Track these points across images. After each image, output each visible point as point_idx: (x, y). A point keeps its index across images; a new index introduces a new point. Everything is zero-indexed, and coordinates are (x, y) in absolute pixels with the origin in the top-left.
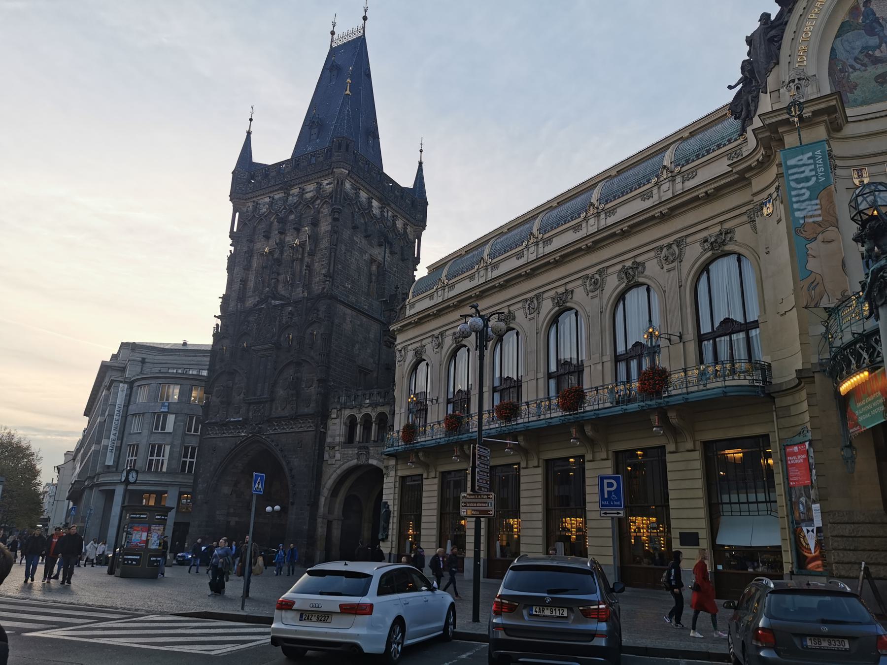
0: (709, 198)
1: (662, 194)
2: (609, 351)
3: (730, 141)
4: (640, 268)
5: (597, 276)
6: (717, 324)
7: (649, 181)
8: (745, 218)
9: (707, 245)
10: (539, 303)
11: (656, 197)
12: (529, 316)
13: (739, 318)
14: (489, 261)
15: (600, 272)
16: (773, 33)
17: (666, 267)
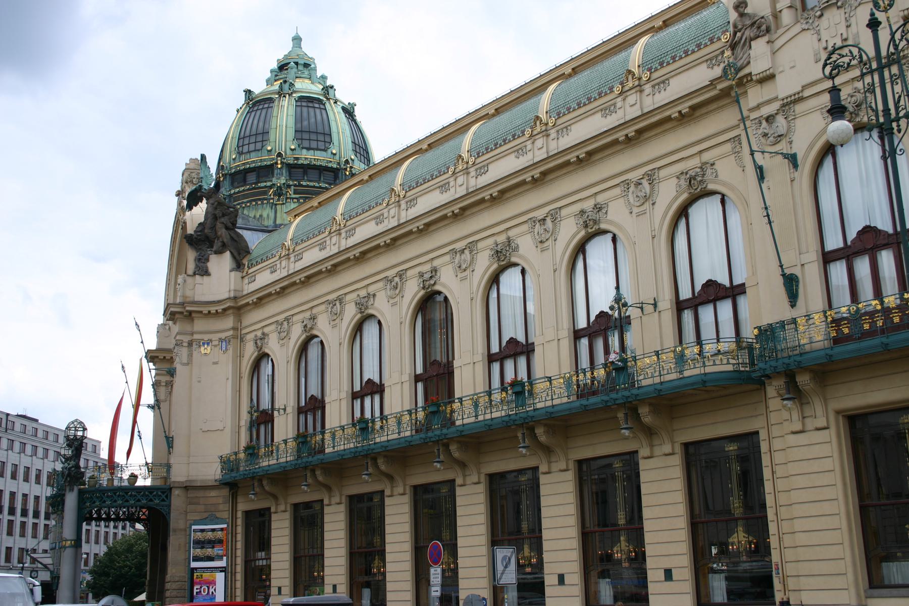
0: (684, 119)
1: (627, 106)
2: (566, 324)
6: (698, 288)
7: (611, 89)
8: (728, 147)
12: (460, 275)
14: (402, 194)
17: (635, 210)
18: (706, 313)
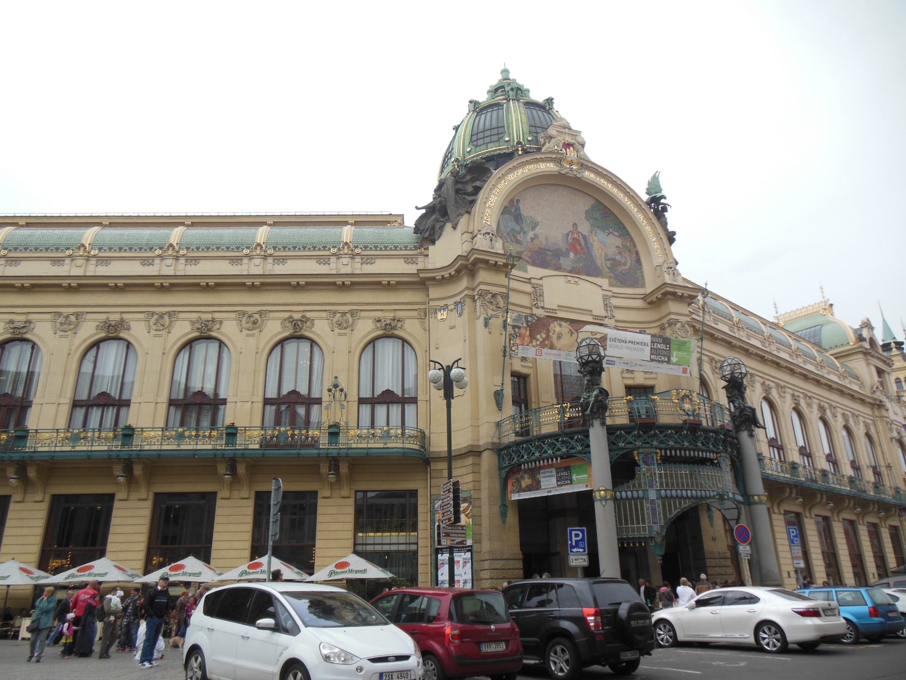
2: (261, 393)
3: (406, 248)
4: (308, 324)
5: (257, 316)
8: (415, 314)
9: (379, 325)
10: (171, 322)
11: (333, 266)
13: (399, 392)
15: (260, 313)
16: (460, 186)
18: (381, 410)
